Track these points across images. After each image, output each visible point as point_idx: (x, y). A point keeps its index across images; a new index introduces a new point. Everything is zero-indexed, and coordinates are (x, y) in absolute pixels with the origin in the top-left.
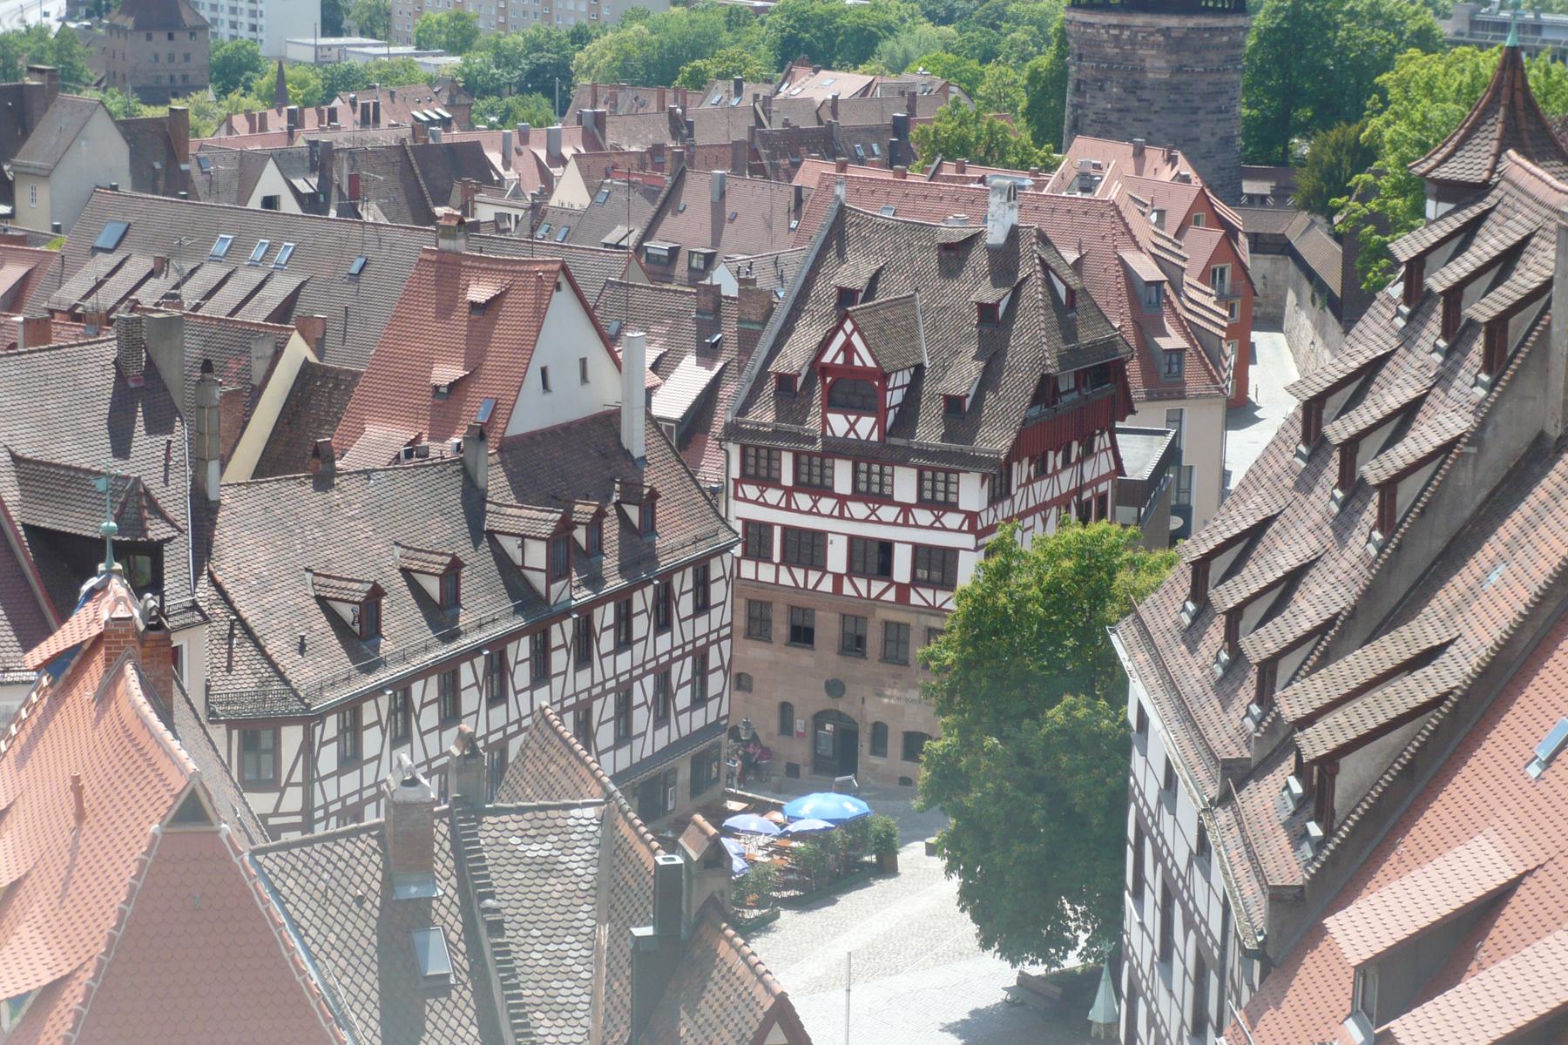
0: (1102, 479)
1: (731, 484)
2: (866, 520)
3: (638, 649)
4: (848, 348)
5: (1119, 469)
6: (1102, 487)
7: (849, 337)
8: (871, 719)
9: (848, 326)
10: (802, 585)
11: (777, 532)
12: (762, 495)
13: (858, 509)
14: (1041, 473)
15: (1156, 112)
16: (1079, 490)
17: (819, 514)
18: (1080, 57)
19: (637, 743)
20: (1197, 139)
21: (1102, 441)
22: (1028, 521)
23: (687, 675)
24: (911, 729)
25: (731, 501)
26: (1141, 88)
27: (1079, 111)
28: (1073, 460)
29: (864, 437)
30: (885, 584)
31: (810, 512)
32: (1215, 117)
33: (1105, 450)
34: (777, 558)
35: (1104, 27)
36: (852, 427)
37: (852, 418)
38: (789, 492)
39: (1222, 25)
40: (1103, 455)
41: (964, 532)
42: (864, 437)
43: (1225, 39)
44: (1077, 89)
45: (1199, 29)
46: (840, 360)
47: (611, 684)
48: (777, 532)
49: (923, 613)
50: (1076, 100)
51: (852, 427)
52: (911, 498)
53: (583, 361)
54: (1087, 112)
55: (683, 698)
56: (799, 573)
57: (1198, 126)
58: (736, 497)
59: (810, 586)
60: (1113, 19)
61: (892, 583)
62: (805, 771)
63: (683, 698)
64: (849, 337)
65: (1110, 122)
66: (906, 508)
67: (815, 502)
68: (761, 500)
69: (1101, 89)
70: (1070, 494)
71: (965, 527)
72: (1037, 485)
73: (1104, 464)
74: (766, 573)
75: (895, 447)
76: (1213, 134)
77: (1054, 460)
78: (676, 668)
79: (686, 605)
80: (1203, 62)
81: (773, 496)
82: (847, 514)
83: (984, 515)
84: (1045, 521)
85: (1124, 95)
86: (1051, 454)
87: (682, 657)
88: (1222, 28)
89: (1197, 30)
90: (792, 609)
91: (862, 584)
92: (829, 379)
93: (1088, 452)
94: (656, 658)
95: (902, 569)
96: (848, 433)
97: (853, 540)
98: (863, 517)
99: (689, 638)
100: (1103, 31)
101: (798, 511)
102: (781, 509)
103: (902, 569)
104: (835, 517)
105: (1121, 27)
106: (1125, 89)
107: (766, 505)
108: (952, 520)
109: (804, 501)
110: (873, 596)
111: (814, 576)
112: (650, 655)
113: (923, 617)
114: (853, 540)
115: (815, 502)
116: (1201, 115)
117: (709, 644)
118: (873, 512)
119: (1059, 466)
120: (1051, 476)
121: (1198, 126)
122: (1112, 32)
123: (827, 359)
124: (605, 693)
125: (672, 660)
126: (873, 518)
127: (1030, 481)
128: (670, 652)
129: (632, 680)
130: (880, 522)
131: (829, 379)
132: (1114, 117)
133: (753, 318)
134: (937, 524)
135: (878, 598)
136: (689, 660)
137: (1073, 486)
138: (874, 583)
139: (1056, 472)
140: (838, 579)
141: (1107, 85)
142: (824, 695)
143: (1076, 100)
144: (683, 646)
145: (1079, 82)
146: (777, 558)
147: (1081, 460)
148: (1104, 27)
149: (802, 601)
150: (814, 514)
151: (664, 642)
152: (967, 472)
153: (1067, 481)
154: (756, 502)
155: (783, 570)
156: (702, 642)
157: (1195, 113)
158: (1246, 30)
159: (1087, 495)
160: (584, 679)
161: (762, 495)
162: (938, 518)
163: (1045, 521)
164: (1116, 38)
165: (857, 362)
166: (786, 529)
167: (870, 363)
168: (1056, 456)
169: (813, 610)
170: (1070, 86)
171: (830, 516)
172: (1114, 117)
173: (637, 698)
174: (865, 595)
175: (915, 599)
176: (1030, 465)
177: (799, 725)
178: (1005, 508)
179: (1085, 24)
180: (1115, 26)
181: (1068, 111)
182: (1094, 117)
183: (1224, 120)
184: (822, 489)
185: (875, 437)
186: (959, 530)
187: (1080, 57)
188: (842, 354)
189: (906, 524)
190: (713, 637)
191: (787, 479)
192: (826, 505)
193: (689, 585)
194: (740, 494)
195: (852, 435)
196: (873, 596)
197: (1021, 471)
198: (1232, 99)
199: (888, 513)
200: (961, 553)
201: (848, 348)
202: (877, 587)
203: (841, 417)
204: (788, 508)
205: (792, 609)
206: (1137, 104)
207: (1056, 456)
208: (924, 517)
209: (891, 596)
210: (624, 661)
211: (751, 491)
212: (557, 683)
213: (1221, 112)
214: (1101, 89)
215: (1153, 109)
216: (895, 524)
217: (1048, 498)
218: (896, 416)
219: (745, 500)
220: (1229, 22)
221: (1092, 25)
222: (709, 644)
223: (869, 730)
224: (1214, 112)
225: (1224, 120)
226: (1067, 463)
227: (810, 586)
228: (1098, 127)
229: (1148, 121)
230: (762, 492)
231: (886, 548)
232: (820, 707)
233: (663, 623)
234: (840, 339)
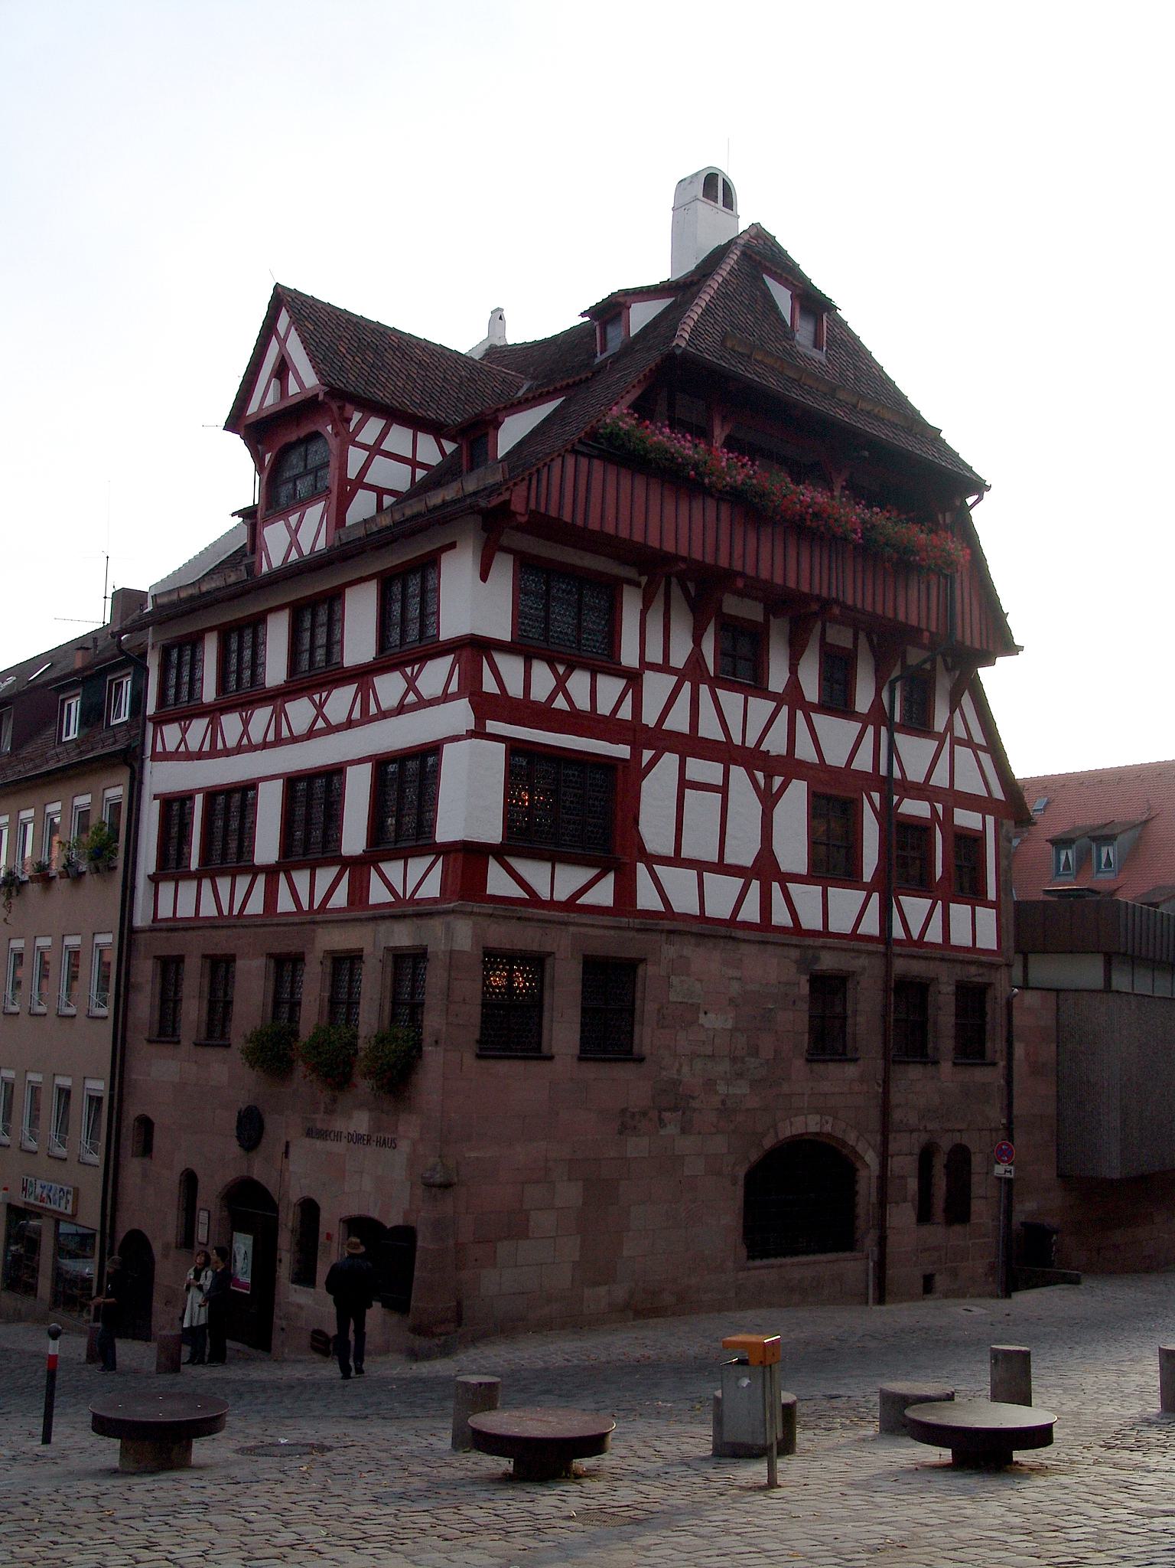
1: (150, 727)
4: (283, 369)
7: (283, 342)
8: (295, 1195)
12: (183, 740)
25: (148, 763)
29: (306, 551)
30: (334, 871)
34: (194, 864)
37: (293, 519)
42: (306, 551)
49: (383, 918)
56: (224, 884)
58: (156, 757)
61: (347, 863)
66: (363, 675)
67: (246, 723)
71: (453, 687)
82: (285, 733)
91: (301, 878)
92: (268, 456)
107: (190, 756)
108: (435, 675)
111: (243, 883)
113: (383, 927)
115: (246, 723)
131: (268, 456)
138: (319, 872)
140: (271, 872)
142: (234, 1147)
146: (194, 864)
149: (221, 943)
152: (452, 546)
165: (293, 388)
166: (212, 795)
167: (311, 380)
174: (306, 907)
175: (378, 893)
176: (697, 640)
185: (321, 544)
186: (446, 698)
191: (209, 693)
194: (159, 749)
202: (325, 876)
211: (171, 733)
219: (166, 756)
227: (235, 912)
230: (184, 731)
232: (230, 1175)
234: (274, 349)
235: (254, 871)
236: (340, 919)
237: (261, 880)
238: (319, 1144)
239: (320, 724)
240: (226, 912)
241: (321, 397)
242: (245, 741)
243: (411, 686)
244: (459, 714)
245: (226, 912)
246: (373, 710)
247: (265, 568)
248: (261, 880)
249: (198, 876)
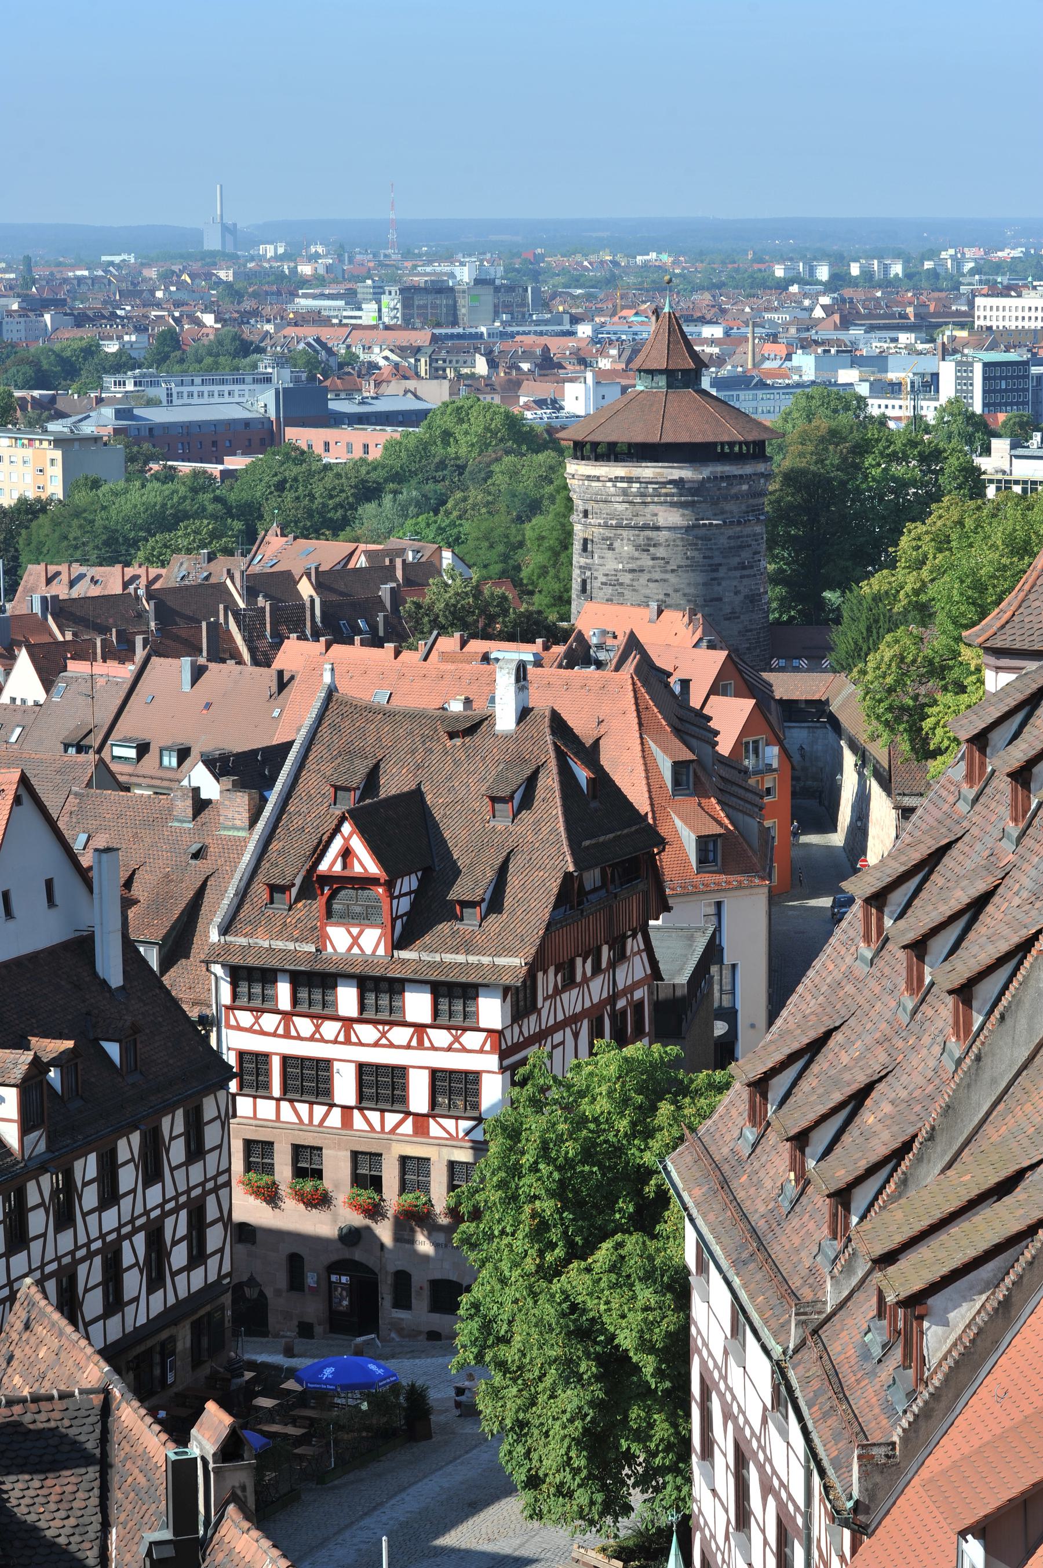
0: (636, 985)
2: (376, 1044)
3: (126, 1203)
4: (347, 853)
5: (656, 973)
6: (638, 994)
7: (347, 840)
8: (391, 1268)
9: (347, 828)
10: (306, 1121)
11: (276, 1064)
12: (257, 1022)
13: (367, 1032)
14: (569, 982)
15: (673, 571)
16: (613, 999)
17: (322, 1040)
18: (586, 514)
19: (130, 1310)
20: (719, 599)
21: (635, 944)
22: (558, 1037)
23: (182, 1230)
24: (438, 1276)
25: (224, 1030)
26: (655, 546)
27: (588, 573)
28: (604, 965)
29: (368, 951)
30: (399, 1116)
31: (312, 1039)
32: (738, 573)
33: (639, 952)
35: (610, 480)
36: (355, 941)
37: (355, 931)
38: (287, 1015)
39: (736, 473)
40: (637, 958)
41: (487, 1052)
42: (368, 951)
43: (745, 487)
44: (585, 549)
45: (716, 478)
46: (338, 867)
47: (97, 1245)
48: (276, 1064)
50: (583, 561)
51: (355, 941)
52: (426, 1018)
53: (49, 884)
54: (596, 574)
55: (179, 1256)
56: (303, 1108)
57: (719, 584)
58: (229, 1026)
59: (316, 1122)
60: (619, 470)
61: (408, 1113)
62: (319, 1330)
63: (179, 1256)
64: (347, 840)
65: (621, 584)
66: (420, 1028)
67: (318, 1027)
68: (256, 1027)
69: (611, 548)
70: (602, 1004)
71: (487, 1047)
72: (565, 996)
73: (637, 968)
74: (266, 1109)
75: (404, 962)
76: (736, 593)
77: (583, 967)
78: (169, 1223)
79: (177, 1152)
80: (722, 513)
81: (270, 1021)
82: (354, 1039)
83: (508, 1033)
84: (576, 1035)
85: (636, 554)
86: (579, 961)
87: (176, 1210)
88: (741, 476)
89: (715, 479)
90: (298, 1150)
91: (374, 1116)
93: (620, 957)
94: (146, 1212)
95: (419, 1098)
96: (350, 948)
97: (362, 1068)
98: (372, 1041)
99: (182, 1188)
100: (609, 484)
101: (299, 1038)
102: (280, 1036)
103: (419, 1098)
104: (341, 1043)
105: (630, 480)
106: (637, 547)
107: (262, 1033)
108: (473, 1039)
109: (304, 1025)
110: (387, 1129)
111: (319, 1110)
112: (139, 1210)
114: (362, 1068)
115: (318, 1027)
116: (722, 572)
117: (205, 1193)
118: (384, 1034)
119: (589, 973)
120: (579, 985)
121: (719, 584)
122: (619, 485)
123: (323, 867)
124: (90, 1256)
125: (165, 1215)
126: (384, 1041)
127: (557, 992)
128: (161, 1206)
129: (121, 1239)
130: (391, 1045)
132: (626, 578)
133: (238, 823)
134: (456, 1045)
135: (393, 1131)
136: (183, 1214)
137: (605, 995)
139: (586, 980)
140: (346, 1109)
141: (617, 544)
143: (583, 561)
144: (176, 1198)
145: (585, 541)
147: (613, 965)
148: (610, 480)
149: (308, 1139)
150: (317, 1040)
151: (154, 1195)
153: (598, 989)
154: (250, 1030)
155: (285, 1105)
156: (198, 1191)
157: (717, 570)
158: (768, 476)
159: (621, 1003)
160: (66, 1241)
161: (257, 1022)
162: (457, 1039)
163: (576, 1035)
164: (625, 492)
166: (285, 1059)
168: (584, 962)
169: (320, 1149)
170: (577, 546)
171: (335, 1042)
172: (626, 578)
173: (127, 1259)
175: (434, 1129)
176: (556, 975)
177: (311, 1280)
178: (531, 1025)
179: (589, 478)
180: (622, 479)
181: (576, 573)
182: (604, 579)
183: (748, 576)
184: (326, 1012)
185: (381, 951)
186: (481, 1051)
187: (586, 514)
188: (340, 860)
189: (421, 1045)
190: (210, 1185)
192: (331, 1029)
193: (179, 1128)
194: (233, 1022)
195: (356, 950)
196: (387, 1129)
197: (547, 981)
198: (755, 553)
199: (400, 1035)
200: (484, 1075)
201: (347, 853)
202: (392, 1119)
203: (342, 930)
204: (287, 1035)
205: (298, 1150)
206: (651, 563)
207: (584, 962)
208: (440, 1037)
209: (408, 1127)
210: (110, 1219)
211: (245, 1018)
212: (36, 1247)
213: (744, 568)
214: (611, 548)
215: (669, 568)
216: (408, 1047)
217: (578, 1009)
218: (404, 926)
219: (239, 1028)
220: (748, 469)
221: (598, 479)
222: (205, 1193)
223: (390, 1280)
224: (736, 569)
225: (748, 576)
226: (597, 970)
227: (316, 1121)
228: (609, 590)
229: (665, 580)
230: (257, 1018)
231: (398, 1075)
232: (335, 1257)
233: (152, 1173)
234: (337, 844)
235: (332, 1105)
236: (404, 1140)
237: (336, 1112)
238: (407, 1246)
239: (384, 1041)
240: (306, 1120)
241: (382, 881)
242: (317, 1036)
243: (457, 1039)
244: (491, 1061)
245: (306, 1121)
246: (427, 1044)
247: (330, 949)
248: (336, 1112)
249: (278, 1100)
